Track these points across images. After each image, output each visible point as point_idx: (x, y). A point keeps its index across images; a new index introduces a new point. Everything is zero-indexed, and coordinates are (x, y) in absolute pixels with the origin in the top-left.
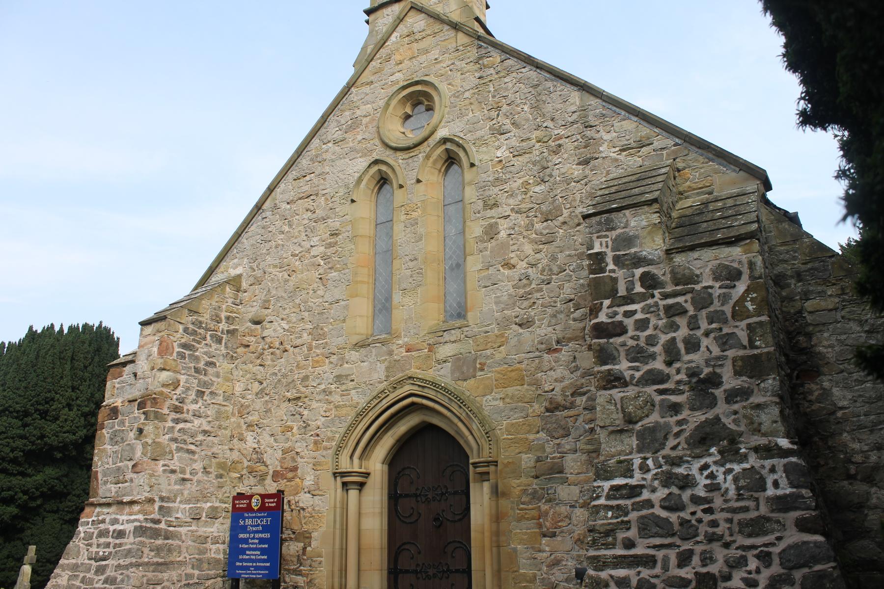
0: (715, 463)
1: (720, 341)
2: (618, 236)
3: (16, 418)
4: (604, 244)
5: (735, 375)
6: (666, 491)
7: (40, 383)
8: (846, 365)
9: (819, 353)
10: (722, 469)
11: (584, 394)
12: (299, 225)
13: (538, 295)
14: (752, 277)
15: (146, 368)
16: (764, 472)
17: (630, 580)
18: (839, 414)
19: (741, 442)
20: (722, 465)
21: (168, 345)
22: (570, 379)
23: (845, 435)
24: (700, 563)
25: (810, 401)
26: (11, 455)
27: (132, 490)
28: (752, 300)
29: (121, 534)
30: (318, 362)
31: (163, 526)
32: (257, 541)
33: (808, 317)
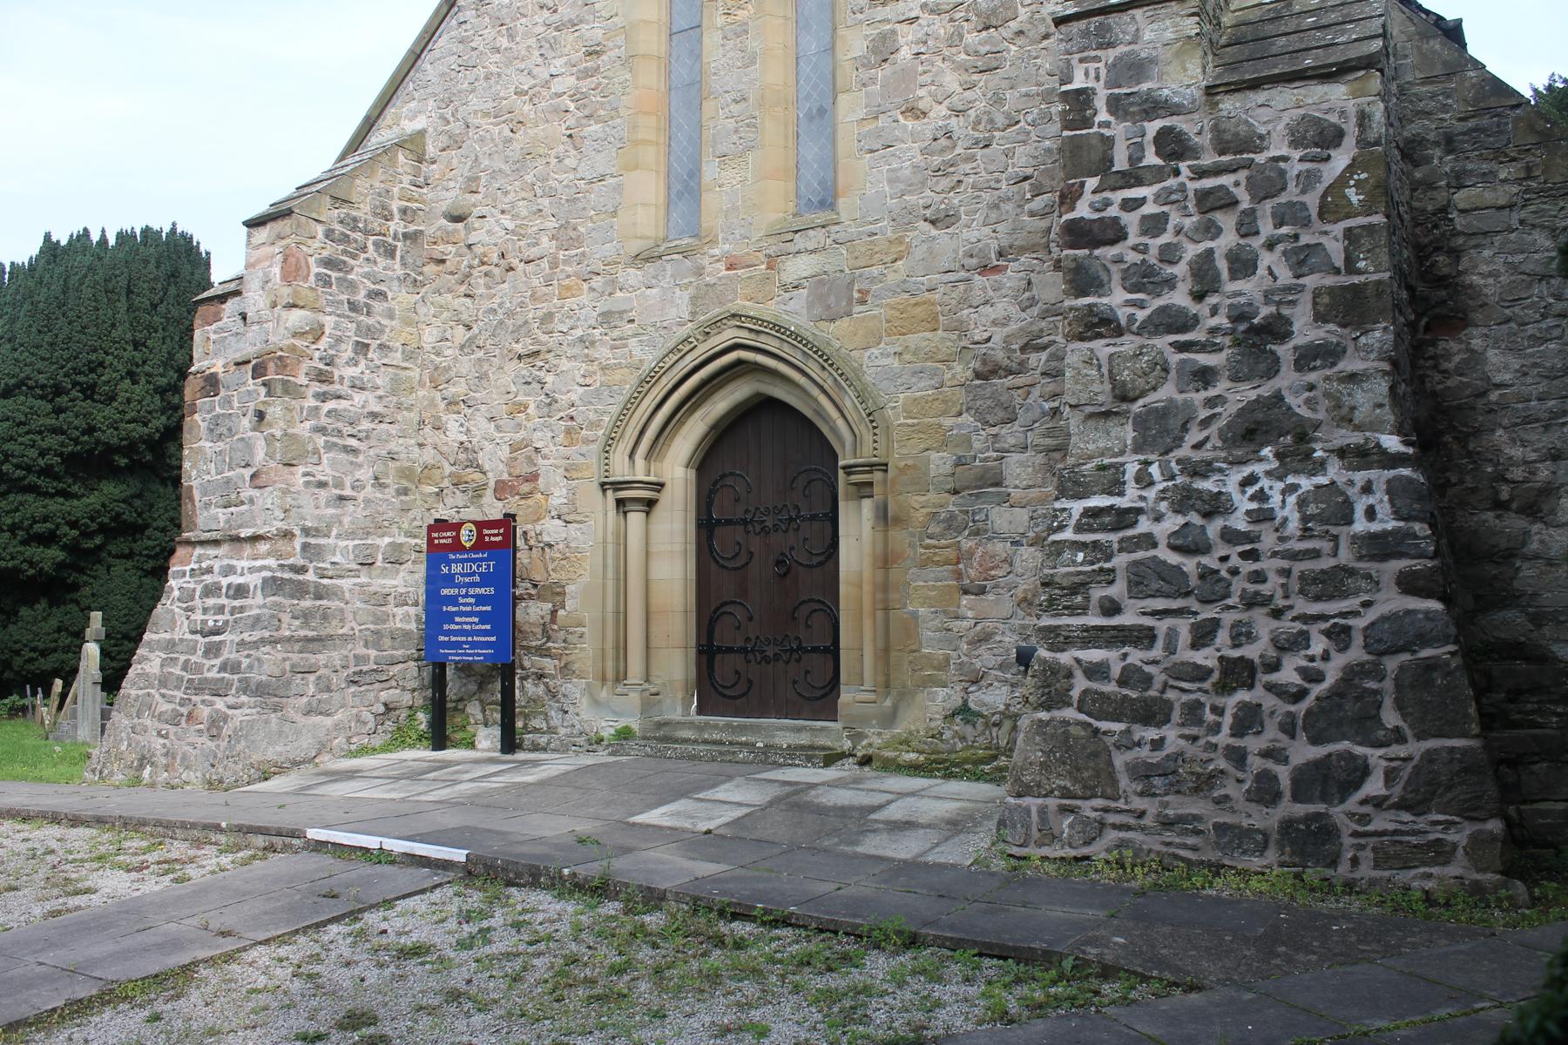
0: (1268, 473)
1: (1294, 259)
2: (1118, 59)
3: (42, 397)
4: (1092, 74)
5: (1316, 320)
6: (1180, 520)
7: (77, 336)
8: (1517, 310)
9: (1471, 286)
10: (1280, 485)
11: (1044, 348)
12: (526, 35)
13: (967, 167)
14: (1362, 142)
15: (262, 305)
16: (1352, 492)
17: (1108, 667)
18: (1494, 396)
19: (1316, 440)
20: (1281, 479)
21: (298, 261)
22: (1020, 321)
23: (1500, 432)
24: (1229, 642)
25: (1445, 372)
26: (41, 462)
27: (254, 518)
28: (1358, 184)
29: (240, 591)
30: (568, 288)
31: (310, 576)
32: (472, 600)
33: (1457, 220)
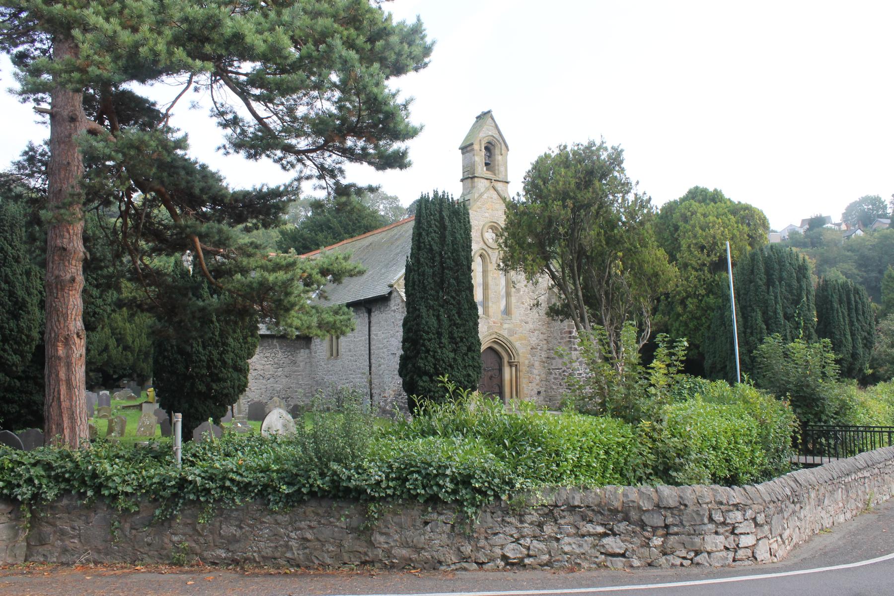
22: (537, 341)
